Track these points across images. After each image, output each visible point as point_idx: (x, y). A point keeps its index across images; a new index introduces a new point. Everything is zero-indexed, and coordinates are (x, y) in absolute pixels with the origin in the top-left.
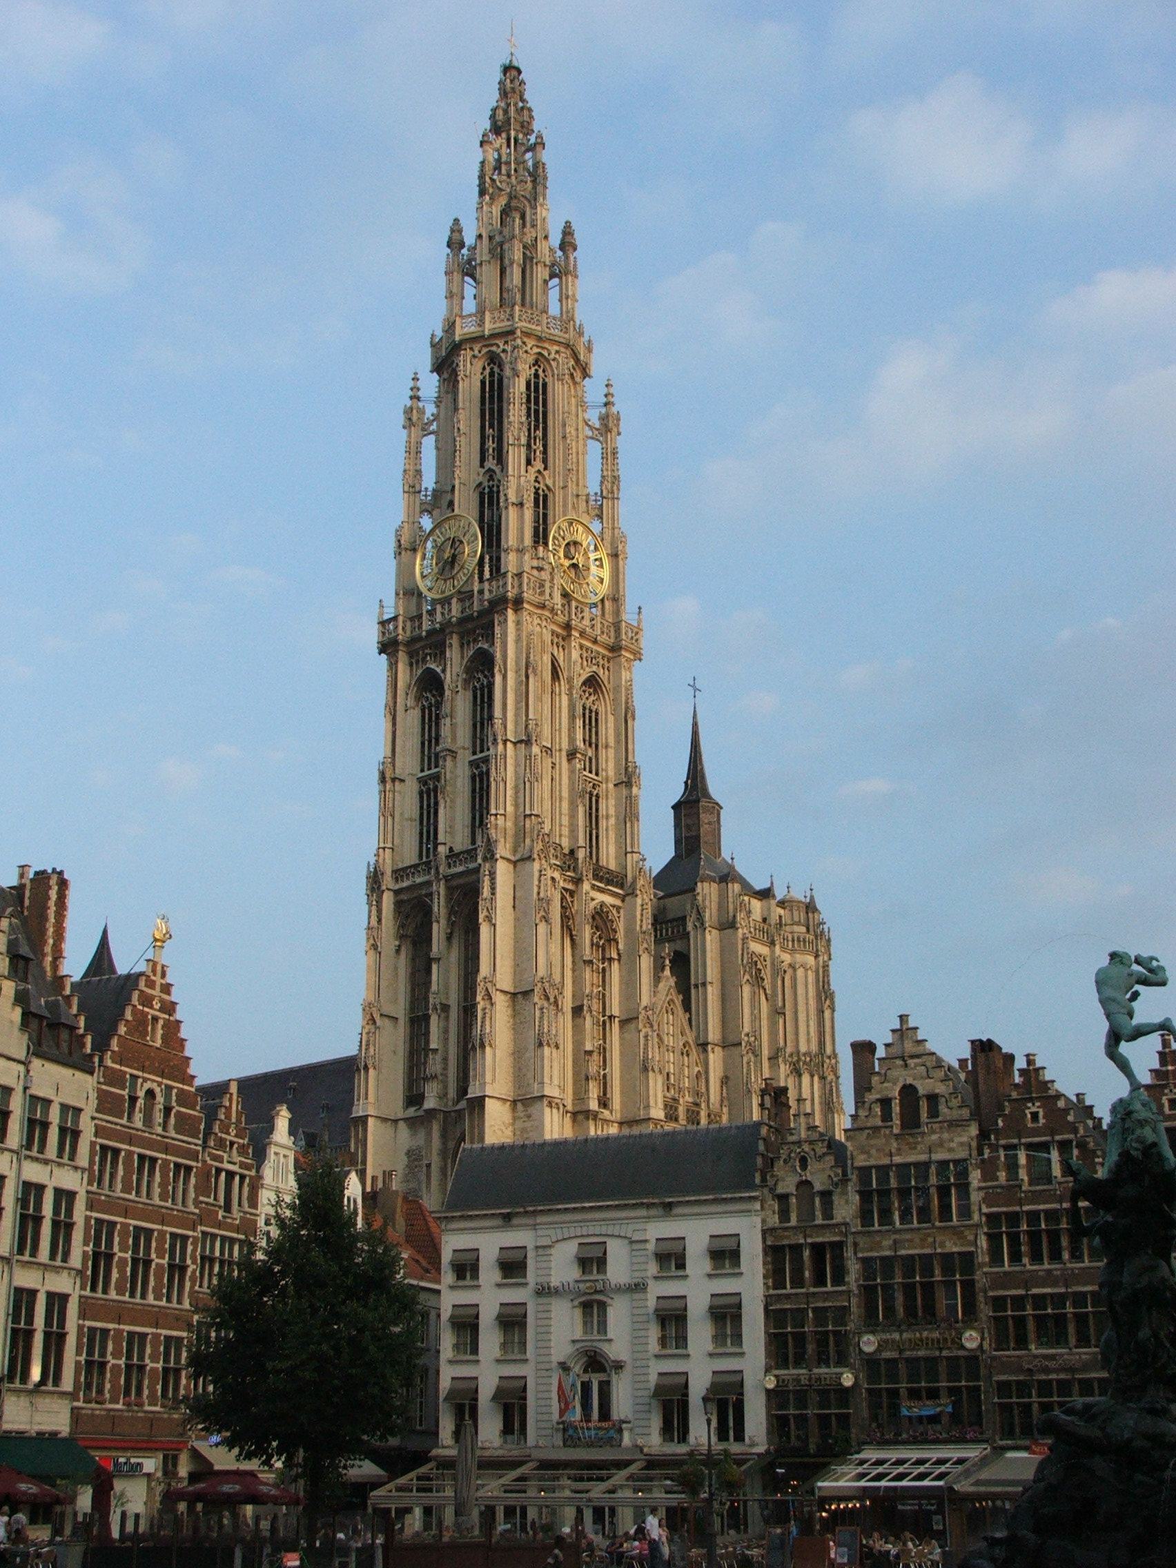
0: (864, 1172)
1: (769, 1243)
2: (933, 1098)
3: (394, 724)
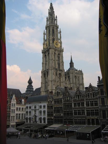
0: (54, 99)
2: (59, 93)
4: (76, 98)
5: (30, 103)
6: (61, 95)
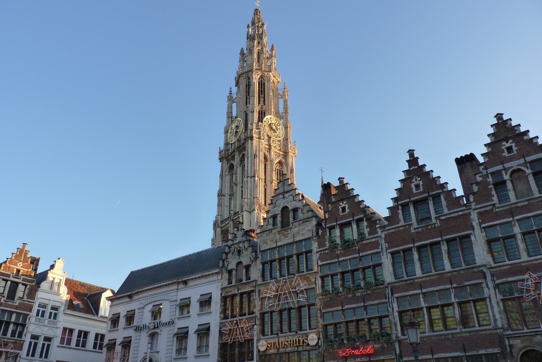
1: (223, 295)
2: (295, 210)
4: (402, 223)
5: (130, 297)
6: (306, 220)
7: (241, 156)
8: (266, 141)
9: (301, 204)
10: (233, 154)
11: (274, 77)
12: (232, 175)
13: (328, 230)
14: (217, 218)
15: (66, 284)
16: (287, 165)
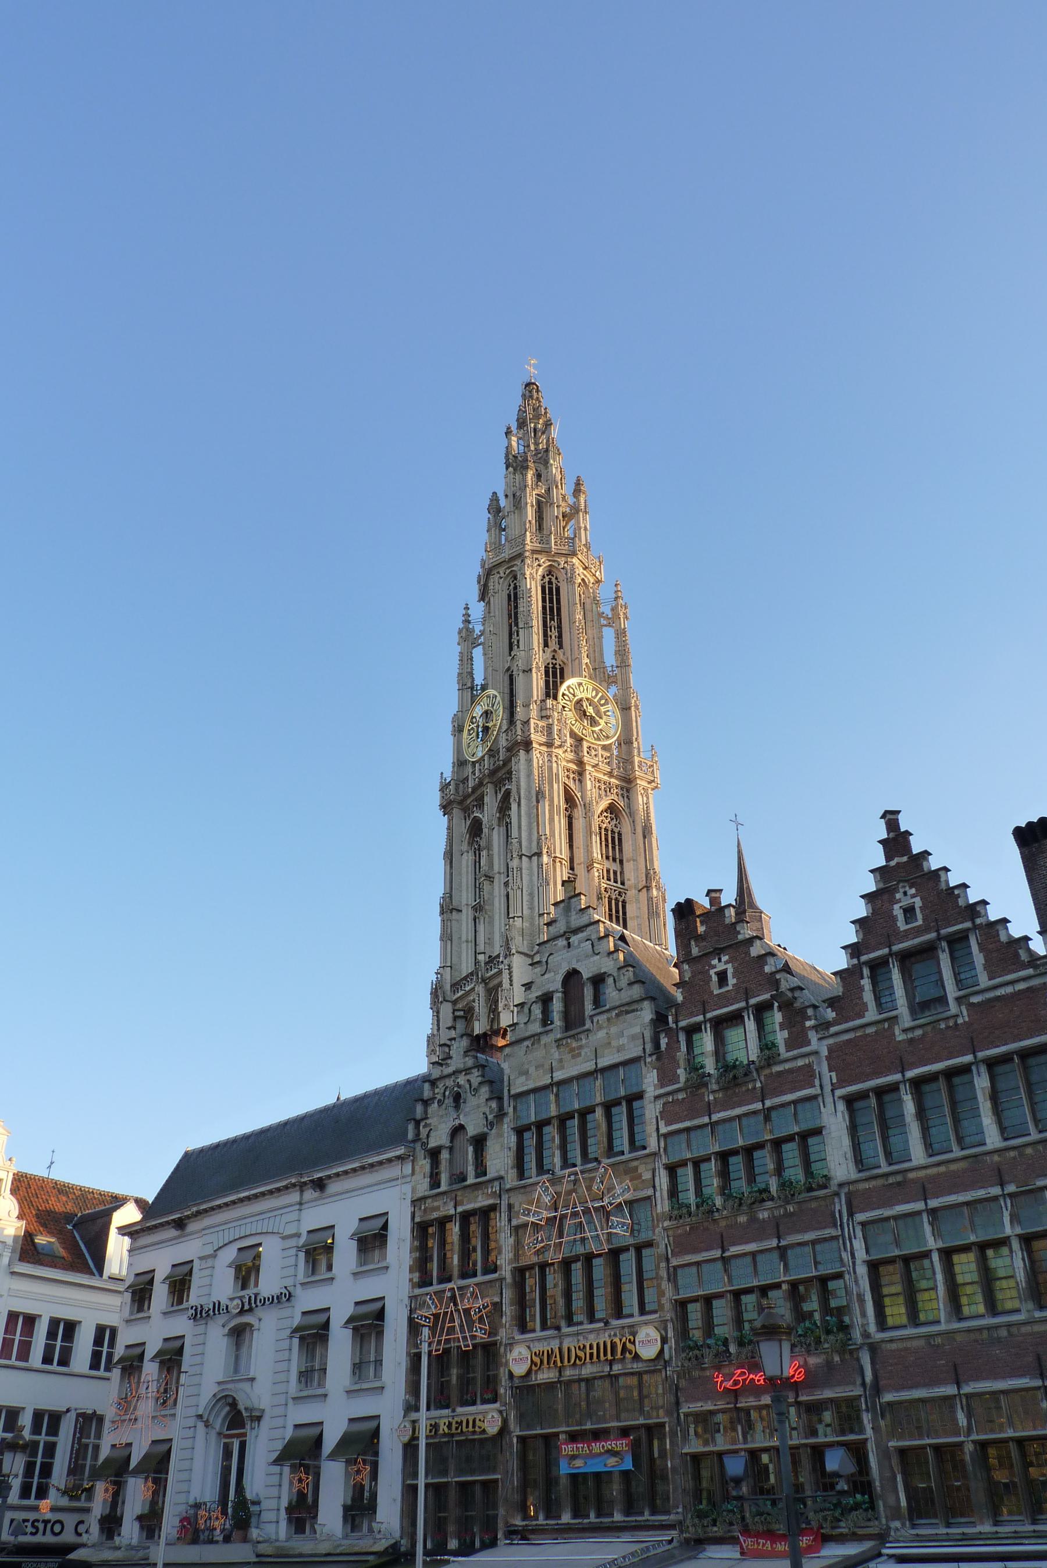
1: (417, 1220)
2: (598, 980)
3: (451, 867)
4: (872, 1014)
5: (180, 1224)
6: (627, 1008)
7: (499, 796)
8: (569, 750)
9: (612, 963)
10: (479, 792)
11: (584, 569)
12: (479, 850)
13: (682, 1037)
14: (442, 976)
15: (14, 1191)
16: (632, 814)
